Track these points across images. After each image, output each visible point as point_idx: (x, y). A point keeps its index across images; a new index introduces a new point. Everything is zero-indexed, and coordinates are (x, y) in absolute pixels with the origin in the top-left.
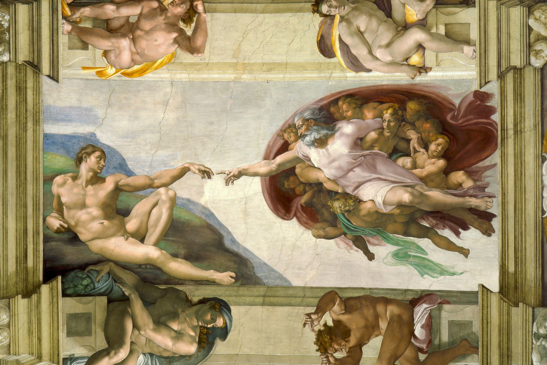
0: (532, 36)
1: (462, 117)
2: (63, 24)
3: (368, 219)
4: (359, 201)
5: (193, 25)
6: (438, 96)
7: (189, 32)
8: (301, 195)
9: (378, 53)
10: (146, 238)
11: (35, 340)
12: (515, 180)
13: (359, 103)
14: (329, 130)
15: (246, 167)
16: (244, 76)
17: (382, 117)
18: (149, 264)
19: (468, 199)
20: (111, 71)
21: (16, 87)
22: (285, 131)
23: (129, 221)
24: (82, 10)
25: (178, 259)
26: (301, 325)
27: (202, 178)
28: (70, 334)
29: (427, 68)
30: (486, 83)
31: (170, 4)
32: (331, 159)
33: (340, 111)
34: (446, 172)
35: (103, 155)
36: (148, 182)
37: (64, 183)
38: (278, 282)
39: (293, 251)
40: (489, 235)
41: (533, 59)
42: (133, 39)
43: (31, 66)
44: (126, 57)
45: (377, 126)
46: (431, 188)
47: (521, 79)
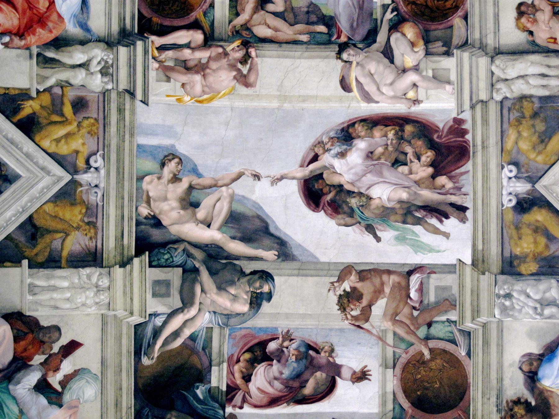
2: (153, 62)
3: (377, 212)
4: (370, 198)
5: (248, 66)
6: (428, 121)
8: (327, 194)
9: (384, 90)
11: (128, 300)
12: (483, 182)
13: (370, 126)
16: (285, 105)
19: (449, 196)
20: (187, 98)
22: (315, 146)
25: (236, 241)
27: (254, 180)
28: (154, 295)
30: (462, 112)
34: (433, 177)
36: (213, 182)
37: (151, 182)
38: (310, 259)
40: (464, 223)
41: (495, 95)
44: (198, 89)
45: (384, 143)
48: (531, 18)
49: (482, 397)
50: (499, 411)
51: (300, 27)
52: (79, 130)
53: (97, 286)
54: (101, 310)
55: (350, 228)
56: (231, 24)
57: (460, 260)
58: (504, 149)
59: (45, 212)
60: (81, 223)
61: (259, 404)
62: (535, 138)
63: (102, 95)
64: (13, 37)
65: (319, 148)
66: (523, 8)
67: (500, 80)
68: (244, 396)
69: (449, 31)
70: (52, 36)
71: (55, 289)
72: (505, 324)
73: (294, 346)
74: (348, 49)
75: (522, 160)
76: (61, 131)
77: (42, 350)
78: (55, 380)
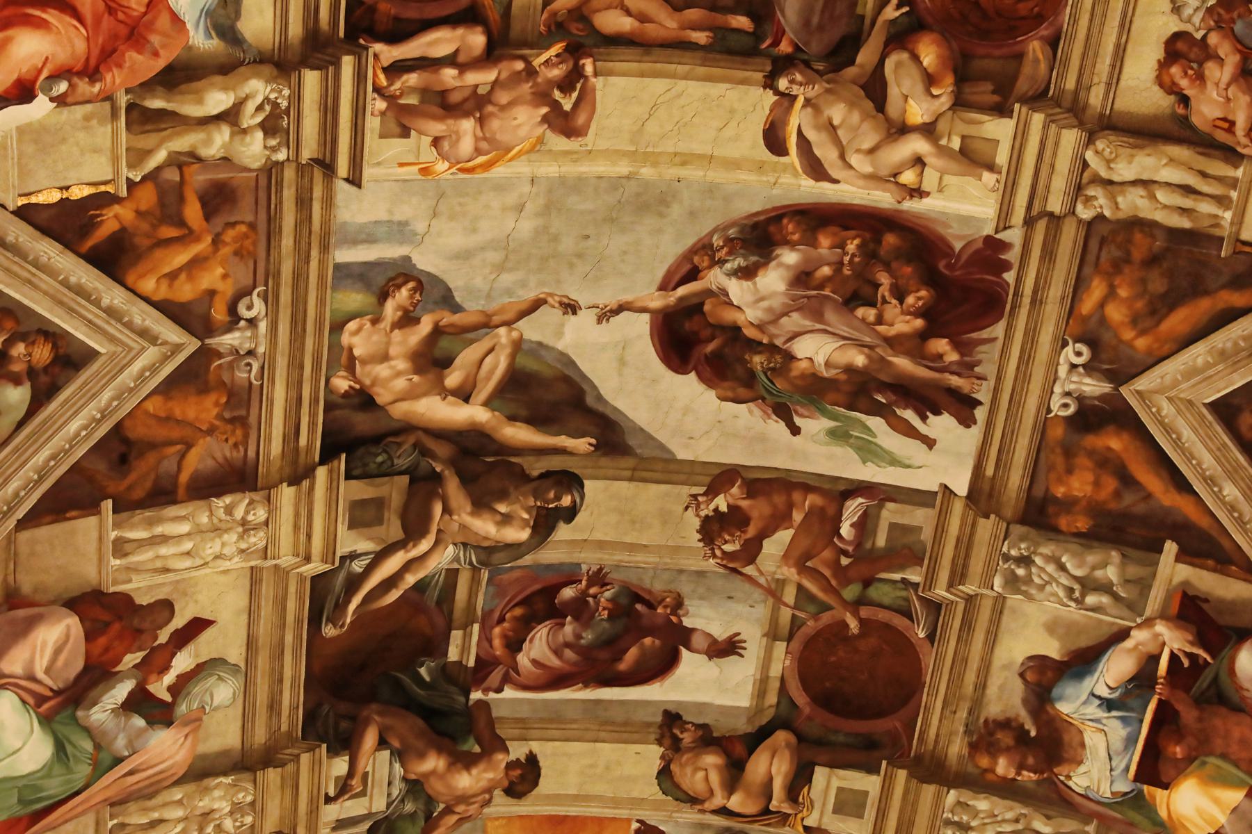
0: (1086, 174)
2: (374, 99)
3: (799, 382)
4: (790, 357)
5: (575, 95)
7: (567, 105)
9: (854, 160)
10: (473, 395)
11: (303, 538)
14: (761, 257)
19: (947, 376)
20: (442, 166)
21: (297, 199)
22: (696, 253)
23: (450, 374)
24: (405, 77)
25: (518, 424)
26: (681, 508)
27: (564, 314)
28: (352, 525)
29: (924, 191)
30: (1005, 228)
31: (543, 64)
33: (784, 232)
34: (924, 336)
35: (420, 287)
38: (657, 453)
39: (684, 415)
40: (968, 426)
41: (1080, 208)
42: (480, 118)
44: (466, 146)
45: (834, 259)
48: (1192, 68)
49: (943, 708)
50: (968, 732)
51: (693, 14)
53: (244, 522)
55: (744, 406)
56: (548, 8)
57: (946, 487)
58: (1076, 312)
59: (147, 413)
60: (217, 423)
61: (531, 683)
62: (1140, 305)
64: (76, 80)
66: (1181, 46)
70: (161, 64)
71: (164, 539)
72: (1009, 603)
73: (608, 594)
75: (1107, 337)
76: (181, 257)
77: (137, 644)
78: (160, 688)
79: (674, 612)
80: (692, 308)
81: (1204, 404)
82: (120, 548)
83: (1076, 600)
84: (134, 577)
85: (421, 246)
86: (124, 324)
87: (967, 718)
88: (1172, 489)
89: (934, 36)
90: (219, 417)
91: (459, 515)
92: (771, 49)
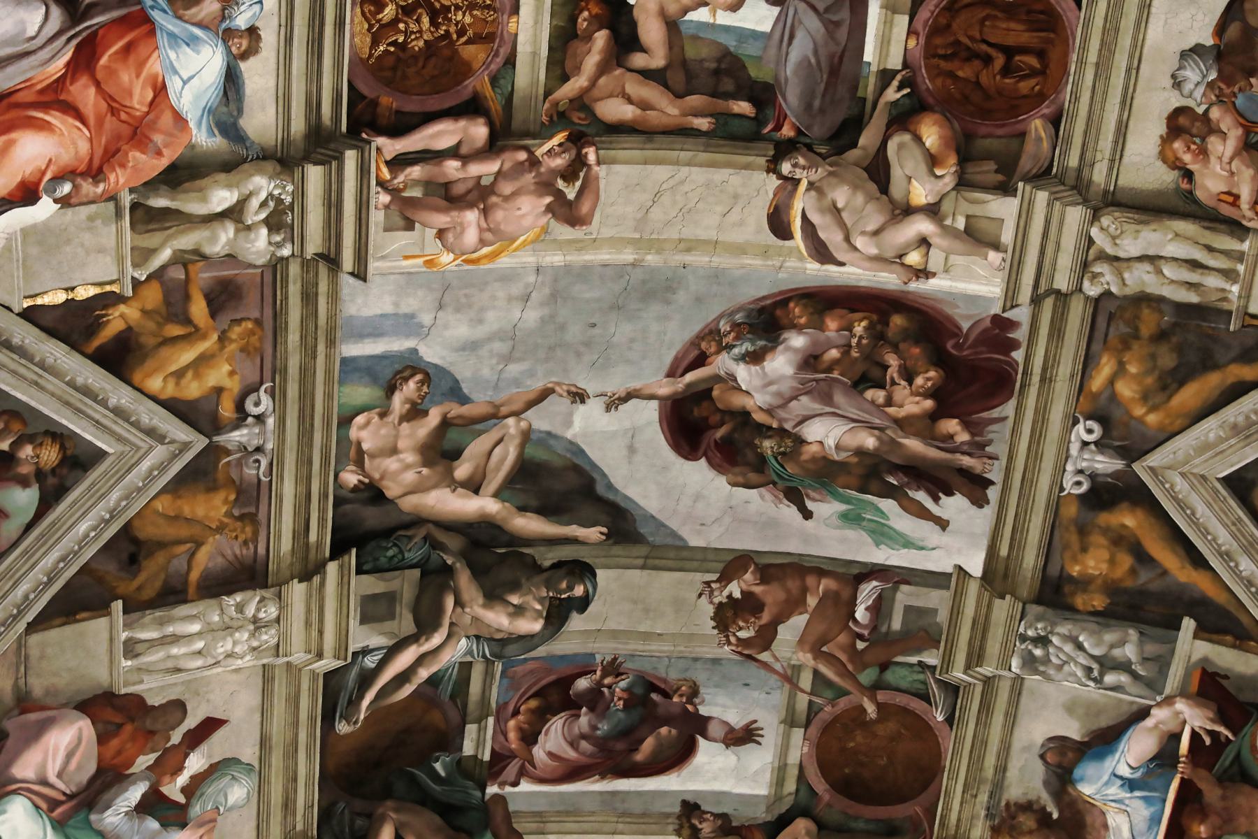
0: (1091, 251)
1: (969, 347)
2: (378, 193)
3: (811, 466)
4: (800, 441)
5: (578, 184)
7: (571, 194)
9: (859, 242)
11: (314, 634)
15: (638, 387)
16: (649, 257)
17: (851, 331)
18: (484, 522)
19: (958, 456)
20: (447, 258)
22: (703, 339)
23: (459, 466)
24: (409, 170)
25: (528, 514)
26: (695, 595)
28: (366, 619)
30: (1013, 307)
32: (767, 381)
34: (934, 416)
35: (427, 379)
37: (368, 423)
38: (669, 541)
40: (981, 507)
41: (1086, 284)
42: (484, 209)
43: (325, 260)
44: (471, 236)
45: (842, 342)
46: (908, 435)
47: (1064, 308)
48: (1194, 143)
49: (963, 792)
50: (990, 815)
51: (695, 100)
52: (222, 348)
53: (255, 620)
54: (261, 659)
57: (960, 568)
58: (1086, 389)
59: (156, 512)
60: (226, 520)
61: (548, 776)
62: (1149, 380)
63: (271, 269)
64: (79, 180)
65: (710, 342)
66: (1182, 120)
67: (1103, 257)
68: (522, 767)
69: (1014, 143)
70: (164, 162)
71: (176, 639)
72: (1027, 684)
73: (623, 684)
74: (795, 154)
75: (1117, 414)
76: (187, 355)
77: (150, 745)
78: (174, 789)
79: (690, 701)
80: (701, 394)
81: (1218, 479)
82: (131, 648)
83: (1095, 680)
84: (146, 678)
85: (429, 338)
86: (132, 424)
87: (989, 802)
88: (1188, 566)
89: (937, 116)
90: (228, 514)
91: (471, 608)
92: (773, 133)
